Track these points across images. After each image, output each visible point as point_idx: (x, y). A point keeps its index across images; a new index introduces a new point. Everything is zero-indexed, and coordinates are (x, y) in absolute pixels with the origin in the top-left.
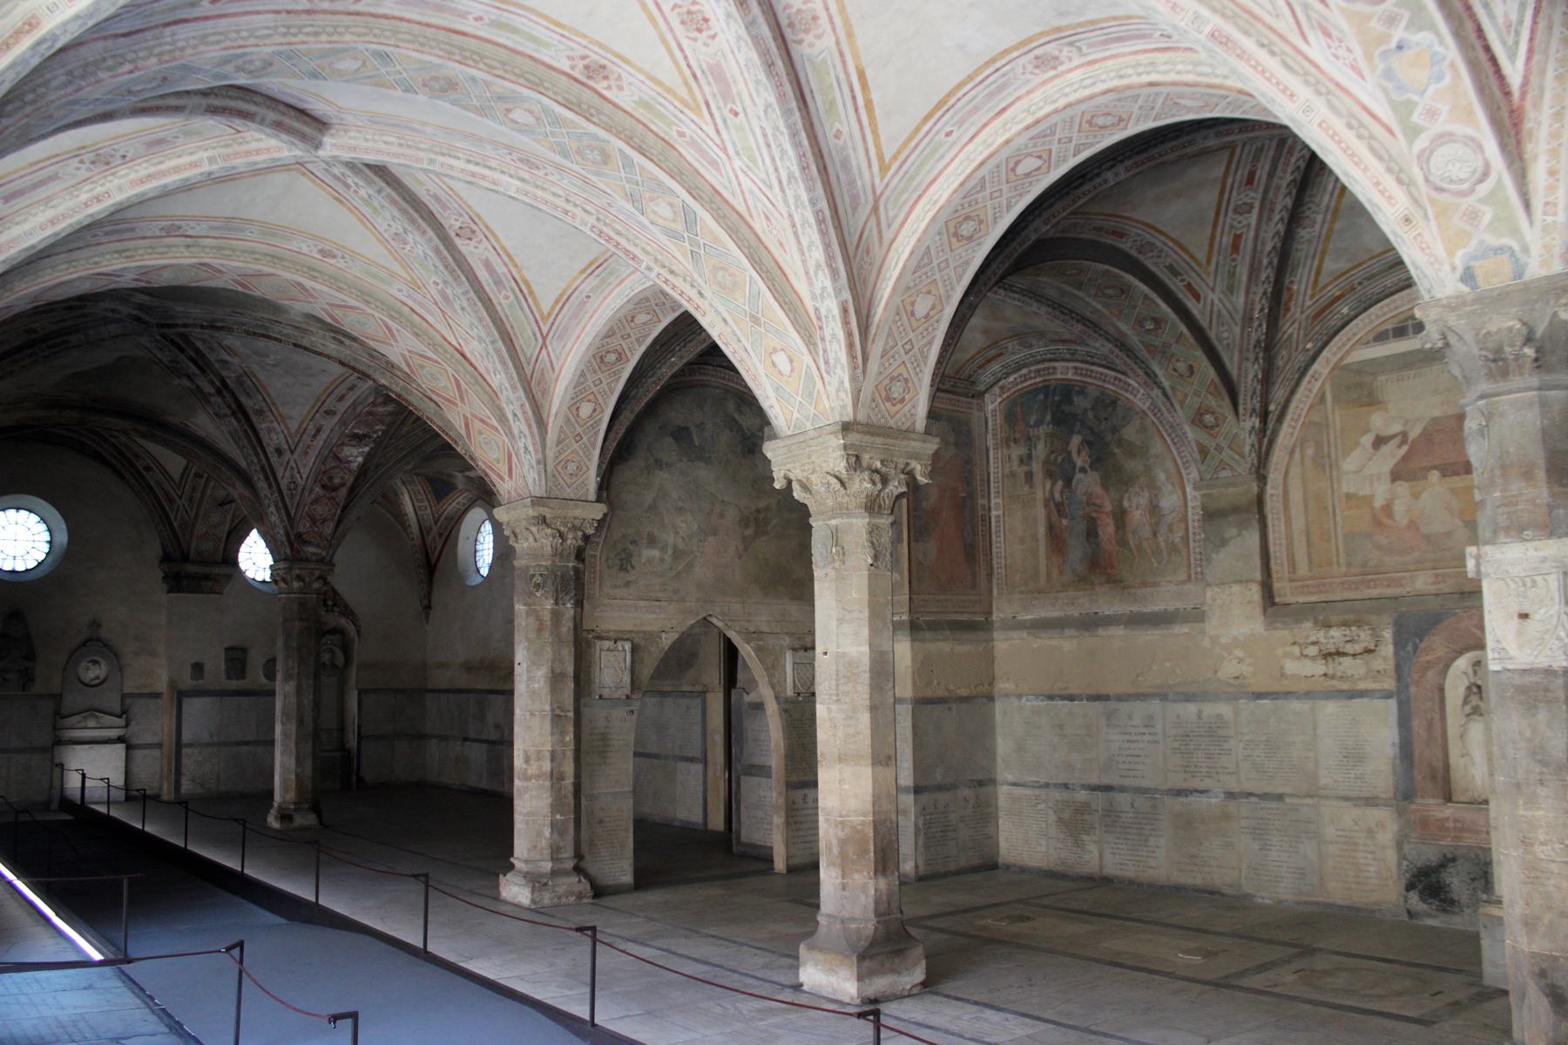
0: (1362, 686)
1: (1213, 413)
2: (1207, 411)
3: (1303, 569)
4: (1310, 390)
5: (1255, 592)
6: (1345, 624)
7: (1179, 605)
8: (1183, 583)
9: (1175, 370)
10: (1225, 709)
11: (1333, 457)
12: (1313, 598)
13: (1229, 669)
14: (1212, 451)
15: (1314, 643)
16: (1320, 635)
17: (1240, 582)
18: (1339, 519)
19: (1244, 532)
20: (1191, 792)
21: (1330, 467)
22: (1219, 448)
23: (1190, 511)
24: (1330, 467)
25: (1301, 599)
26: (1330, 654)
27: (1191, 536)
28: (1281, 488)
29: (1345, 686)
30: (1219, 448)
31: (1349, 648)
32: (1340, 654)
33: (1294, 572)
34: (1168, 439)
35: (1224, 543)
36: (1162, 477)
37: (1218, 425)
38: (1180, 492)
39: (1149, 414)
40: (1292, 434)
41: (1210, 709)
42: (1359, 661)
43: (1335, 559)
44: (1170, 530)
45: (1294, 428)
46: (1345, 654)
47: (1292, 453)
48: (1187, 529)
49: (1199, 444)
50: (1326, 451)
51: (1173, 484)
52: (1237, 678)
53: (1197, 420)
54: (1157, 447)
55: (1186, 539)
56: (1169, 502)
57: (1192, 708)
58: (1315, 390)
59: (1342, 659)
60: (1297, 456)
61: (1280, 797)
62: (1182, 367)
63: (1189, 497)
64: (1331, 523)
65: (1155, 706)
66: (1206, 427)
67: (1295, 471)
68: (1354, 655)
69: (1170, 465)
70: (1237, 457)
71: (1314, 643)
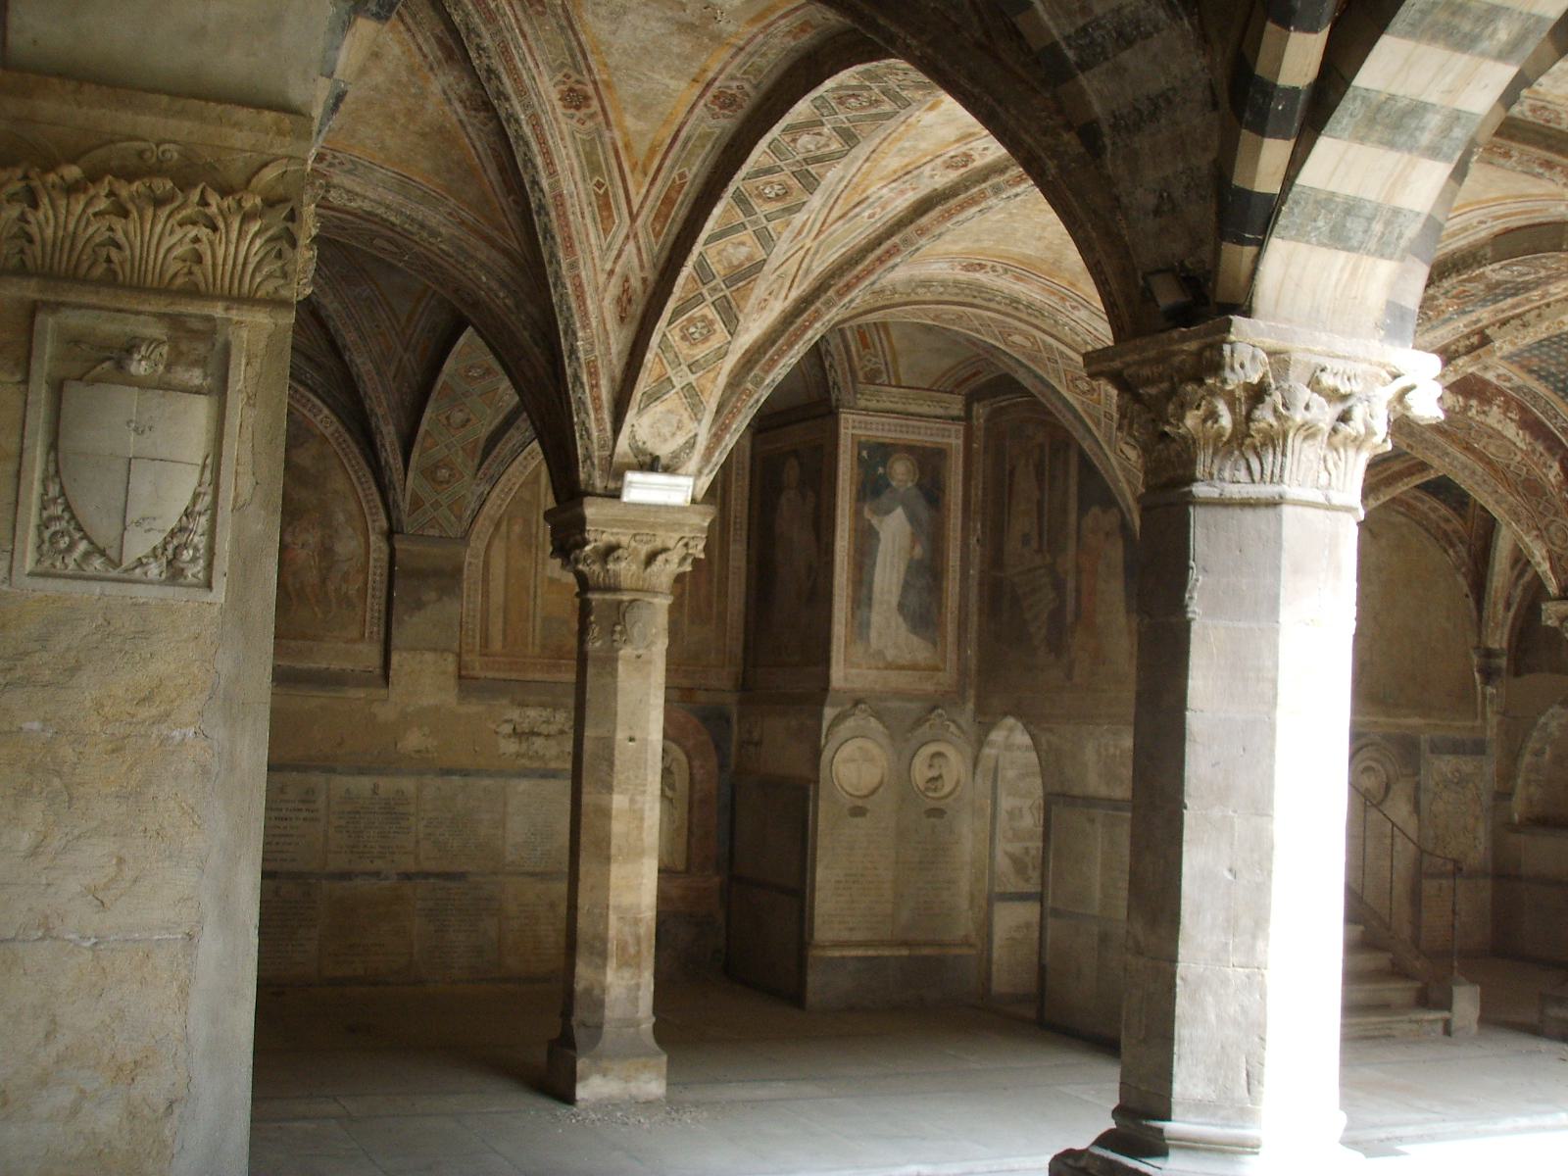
0: (553, 765)
1: (452, 469)
2: (445, 466)
3: (497, 645)
4: (525, 467)
5: (450, 663)
6: (543, 705)
7: (348, 666)
8: (353, 641)
9: (448, 418)
10: (408, 784)
11: (541, 539)
12: (502, 675)
13: (413, 740)
14: (428, 505)
15: (506, 721)
16: (514, 714)
17: (435, 650)
18: (539, 601)
19: (445, 598)
20: (357, 876)
21: (537, 547)
22: (436, 505)
23: (371, 563)
24: (537, 547)
25: (490, 675)
26: (523, 733)
27: (370, 591)
28: (482, 558)
29: (536, 765)
30: (436, 505)
31: (544, 729)
32: (533, 733)
33: (487, 647)
34: (353, 477)
35: (419, 605)
36: (341, 517)
37: (448, 482)
38: (362, 540)
39: (331, 441)
40: (500, 506)
41: (387, 784)
42: (553, 742)
43: (530, 639)
44: (345, 578)
45: (503, 500)
46: (539, 734)
47: (498, 526)
48: (366, 584)
49: (415, 495)
50: (534, 531)
51: (354, 529)
52: (419, 751)
53: (429, 473)
54: (338, 483)
55: (363, 592)
56: (347, 546)
57: (365, 783)
58: (530, 469)
59: (534, 739)
60: (504, 528)
61: (461, 876)
62: (458, 417)
63: (373, 547)
64: (532, 603)
65: (317, 779)
66: (434, 480)
67: (499, 546)
68: (548, 736)
69: (352, 506)
70: (453, 518)
71: (506, 721)
